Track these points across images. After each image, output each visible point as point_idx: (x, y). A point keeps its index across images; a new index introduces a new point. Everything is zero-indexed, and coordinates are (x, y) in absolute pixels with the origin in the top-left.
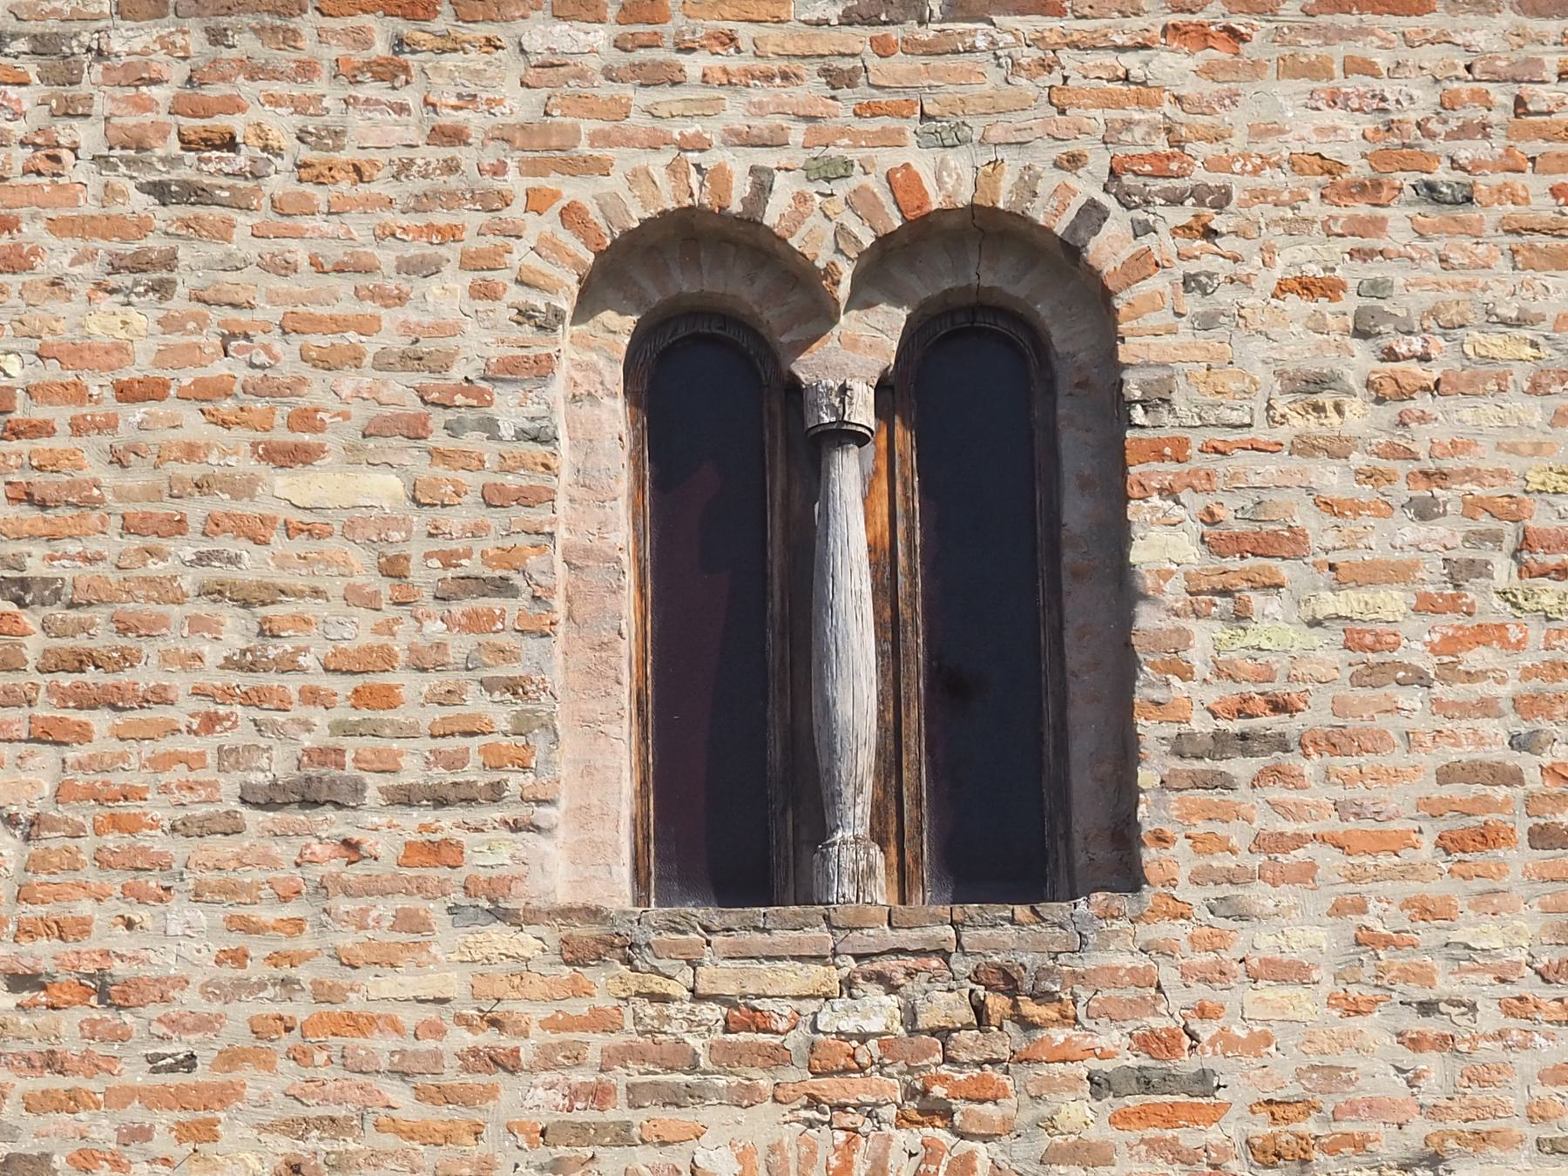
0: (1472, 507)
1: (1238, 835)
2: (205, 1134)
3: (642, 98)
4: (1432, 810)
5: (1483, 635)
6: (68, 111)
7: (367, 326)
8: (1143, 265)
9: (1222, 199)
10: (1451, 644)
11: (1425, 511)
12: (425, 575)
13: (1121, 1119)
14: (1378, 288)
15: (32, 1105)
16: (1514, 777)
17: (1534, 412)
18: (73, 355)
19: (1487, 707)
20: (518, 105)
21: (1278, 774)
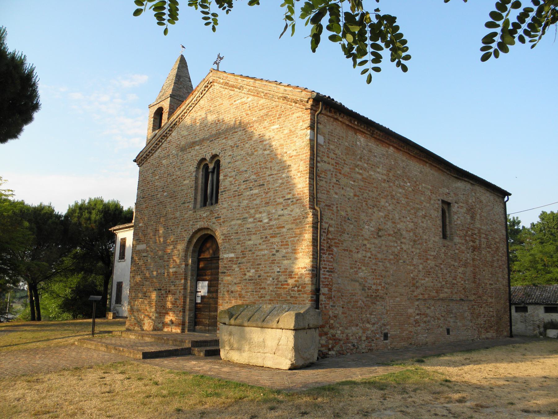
0: (237, 170)
1: (223, 198)
2: (178, 227)
3: (200, 150)
4: (233, 194)
5: (237, 180)
6: (178, 159)
7: (188, 170)
8: (222, 156)
9: (226, 150)
10: (235, 181)
11: (234, 171)
12: (189, 187)
13: (216, 220)
14: (233, 155)
15: (173, 226)
16: (237, 191)
17: (240, 162)
18: (177, 176)
19: (236, 186)
20: (195, 153)
21: (225, 193)
